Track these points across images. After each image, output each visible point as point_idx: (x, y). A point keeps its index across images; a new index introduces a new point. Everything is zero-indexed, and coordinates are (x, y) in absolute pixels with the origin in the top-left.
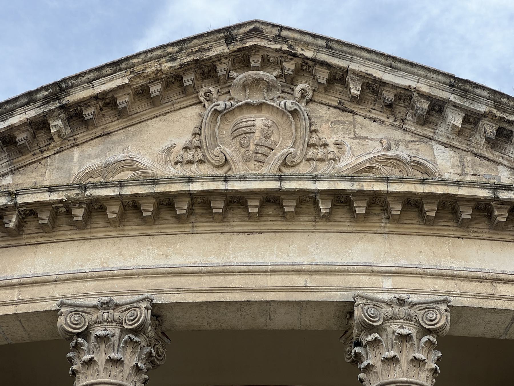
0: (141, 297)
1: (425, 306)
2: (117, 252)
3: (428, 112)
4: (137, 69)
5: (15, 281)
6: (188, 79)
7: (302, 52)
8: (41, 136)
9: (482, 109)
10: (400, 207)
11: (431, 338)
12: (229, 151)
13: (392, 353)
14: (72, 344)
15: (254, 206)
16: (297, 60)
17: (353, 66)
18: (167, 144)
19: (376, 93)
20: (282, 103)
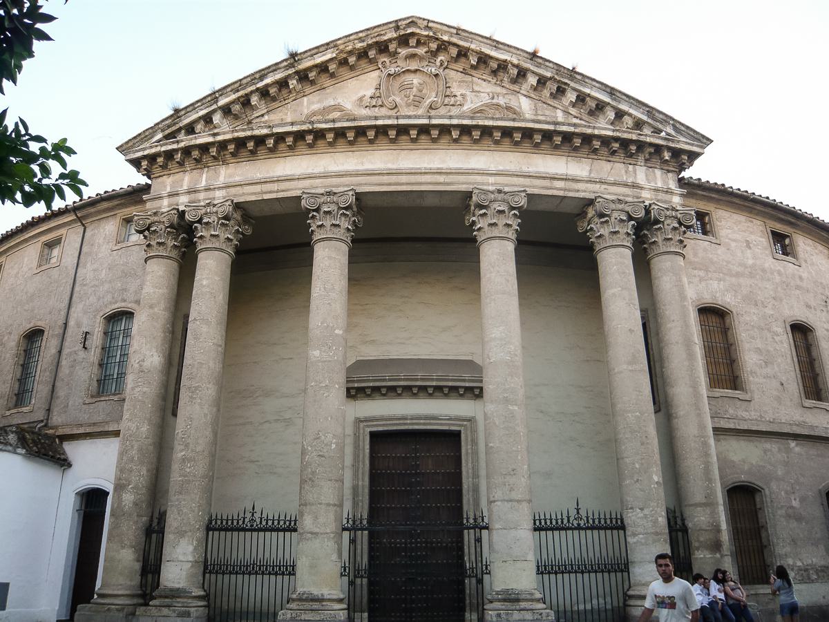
0: (349, 188)
1: (513, 194)
2: (333, 162)
3: (517, 76)
4: (341, 47)
5: (275, 179)
6: (372, 54)
7: (440, 37)
8: (284, 92)
9: (549, 75)
10: (500, 135)
11: (516, 212)
12: (398, 100)
13: (494, 221)
14: (310, 215)
15: (414, 133)
16: (438, 42)
17: (473, 46)
18: (360, 94)
19: (485, 63)
20: (430, 69)
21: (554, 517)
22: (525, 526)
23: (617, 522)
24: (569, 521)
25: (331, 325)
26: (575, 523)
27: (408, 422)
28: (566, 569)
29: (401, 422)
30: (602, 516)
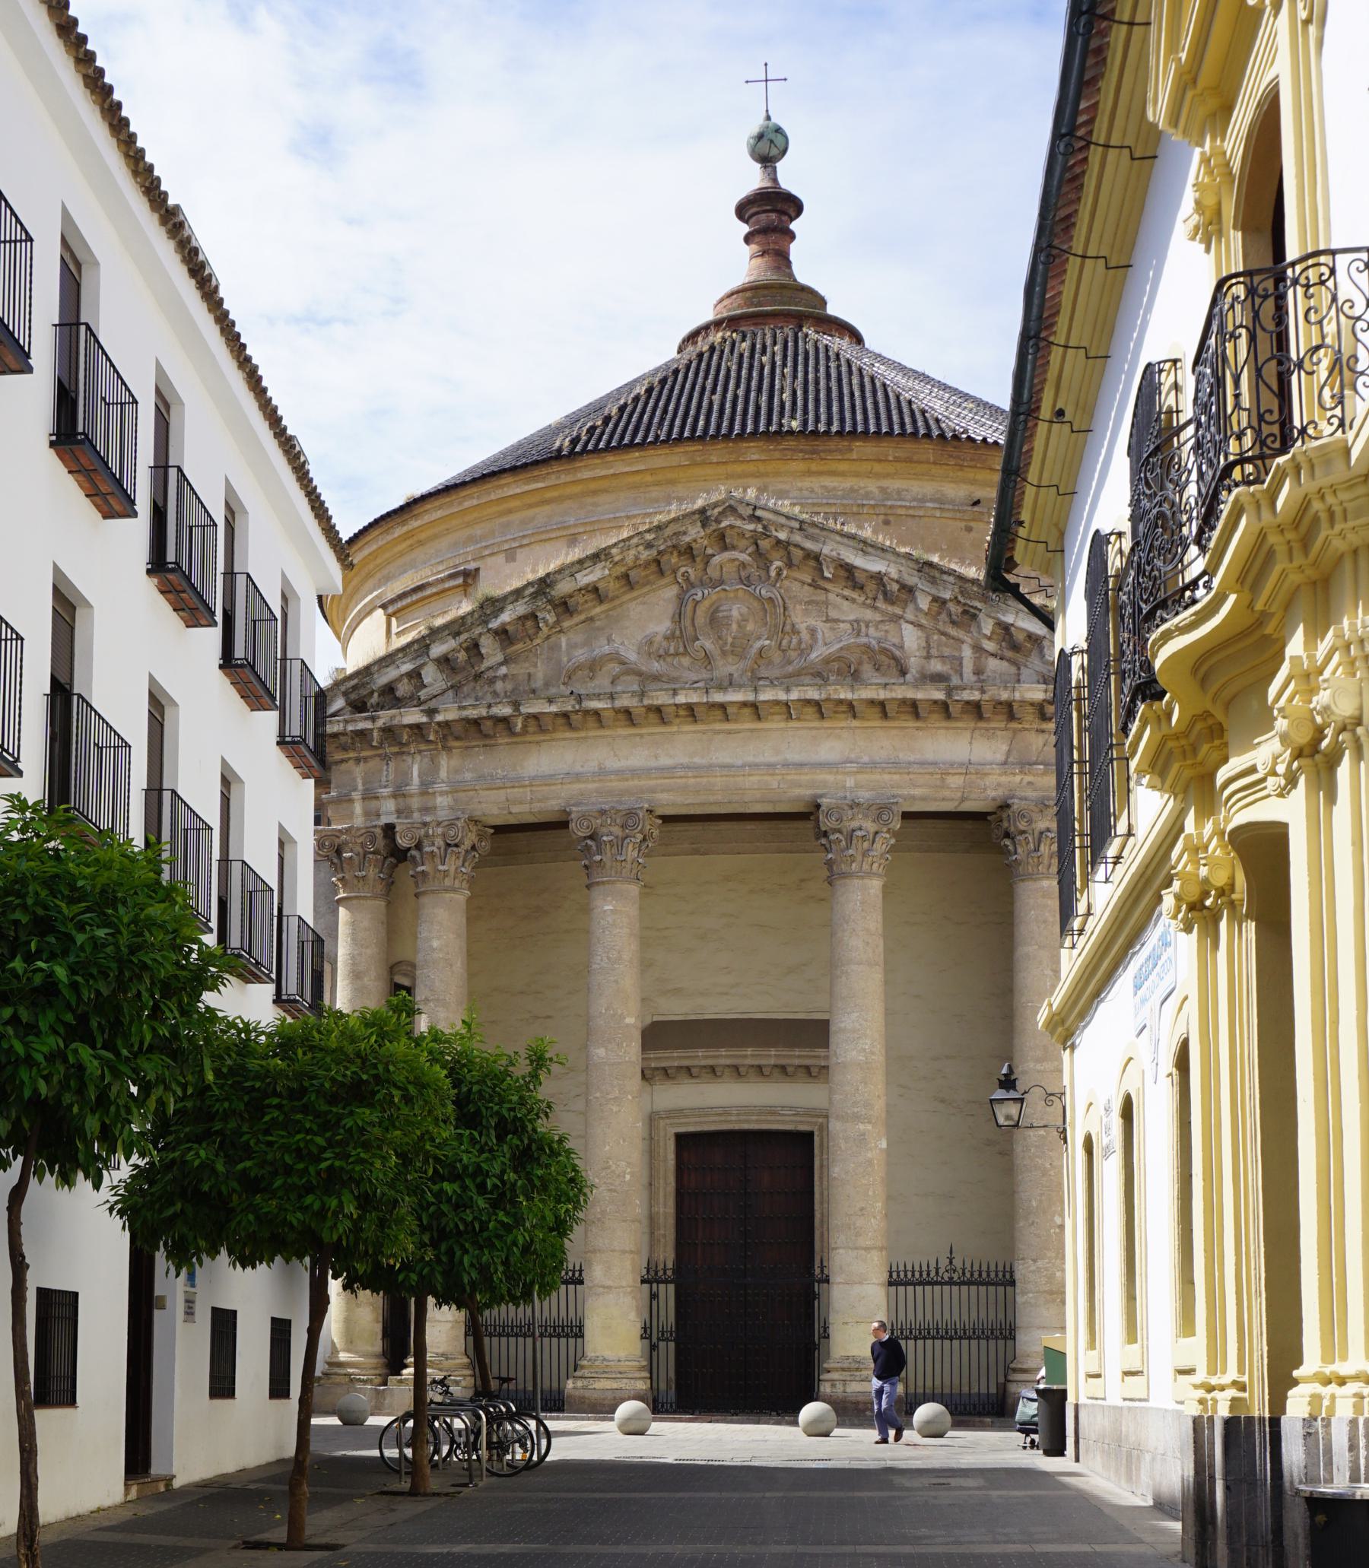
4: (617, 559)
12: (708, 645)
21: (917, 1268)
22: (875, 1281)
23: (1004, 1276)
24: (937, 1273)
25: (620, 1012)
26: (946, 1277)
27: (733, 1118)
28: (929, 1333)
29: (723, 1118)
30: (984, 1268)
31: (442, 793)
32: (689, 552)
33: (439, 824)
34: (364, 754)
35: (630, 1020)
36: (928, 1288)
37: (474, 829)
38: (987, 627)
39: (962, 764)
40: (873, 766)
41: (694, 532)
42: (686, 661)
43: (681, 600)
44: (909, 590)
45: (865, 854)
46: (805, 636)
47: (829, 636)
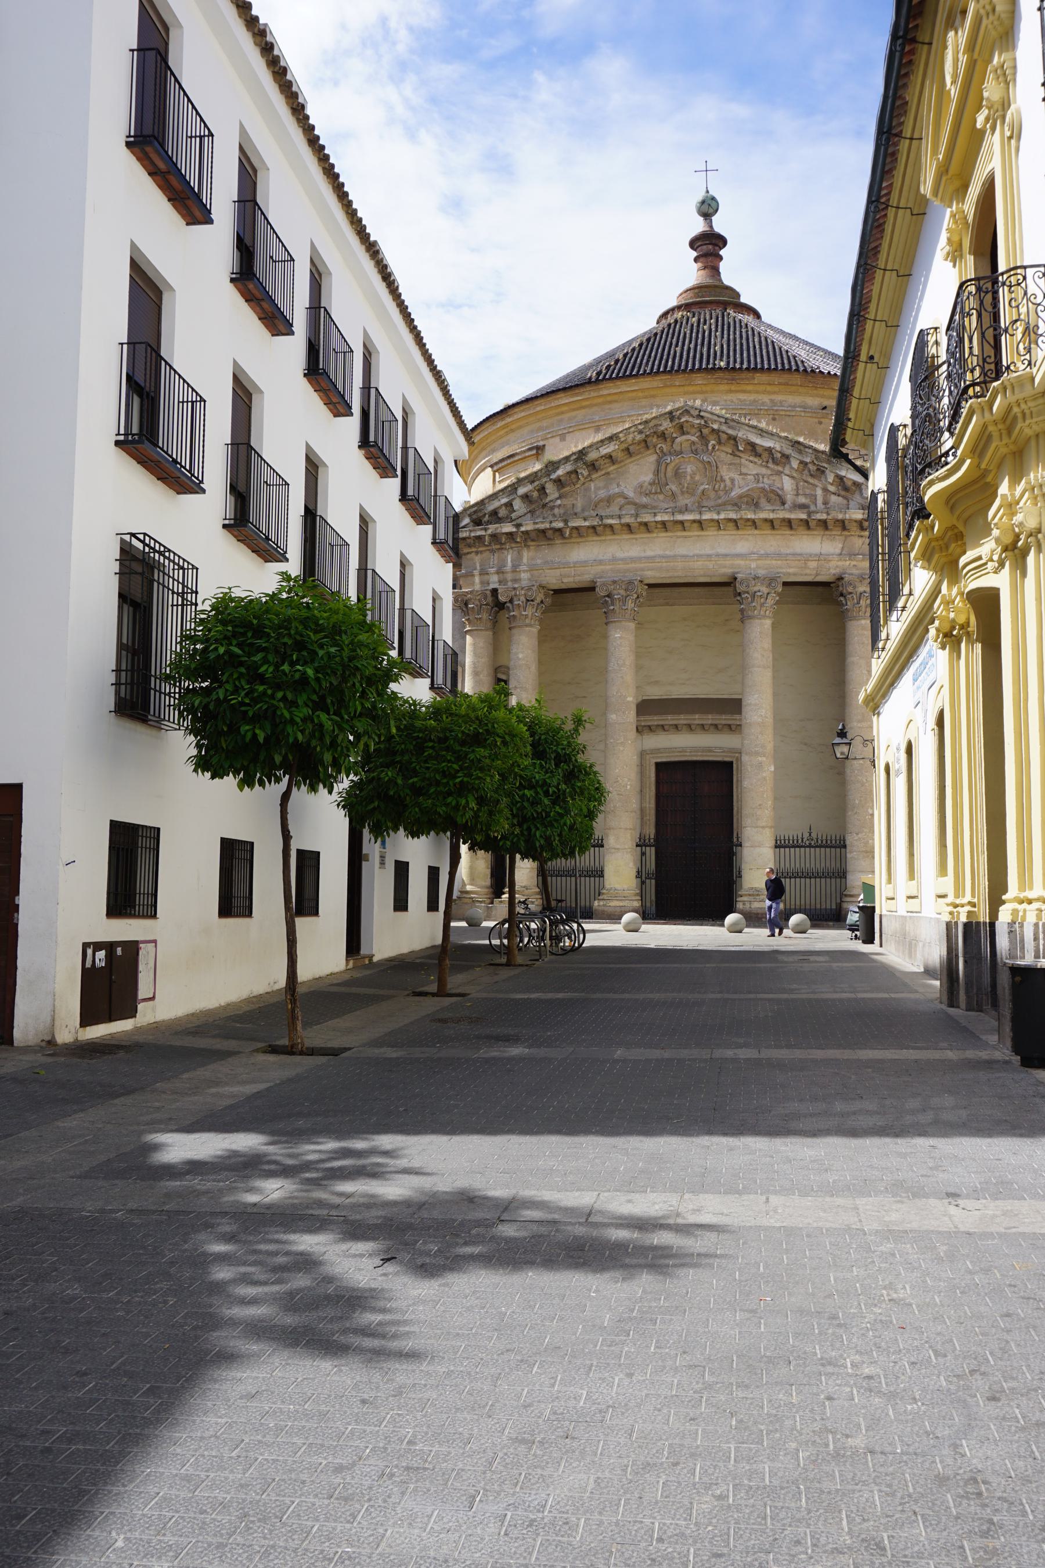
12: (674, 488)
31: (524, 571)
32: (663, 436)
33: (522, 589)
34: (481, 549)
35: (630, 699)
36: (797, 849)
37: (542, 591)
38: (831, 478)
39: (816, 555)
40: (767, 556)
41: (666, 425)
42: (661, 497)
43: (658, 463)
44: (787, 457)
45: (762, 605)
46: (728, 483)
47: (742, 482)
